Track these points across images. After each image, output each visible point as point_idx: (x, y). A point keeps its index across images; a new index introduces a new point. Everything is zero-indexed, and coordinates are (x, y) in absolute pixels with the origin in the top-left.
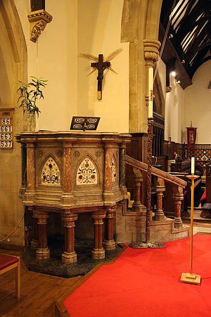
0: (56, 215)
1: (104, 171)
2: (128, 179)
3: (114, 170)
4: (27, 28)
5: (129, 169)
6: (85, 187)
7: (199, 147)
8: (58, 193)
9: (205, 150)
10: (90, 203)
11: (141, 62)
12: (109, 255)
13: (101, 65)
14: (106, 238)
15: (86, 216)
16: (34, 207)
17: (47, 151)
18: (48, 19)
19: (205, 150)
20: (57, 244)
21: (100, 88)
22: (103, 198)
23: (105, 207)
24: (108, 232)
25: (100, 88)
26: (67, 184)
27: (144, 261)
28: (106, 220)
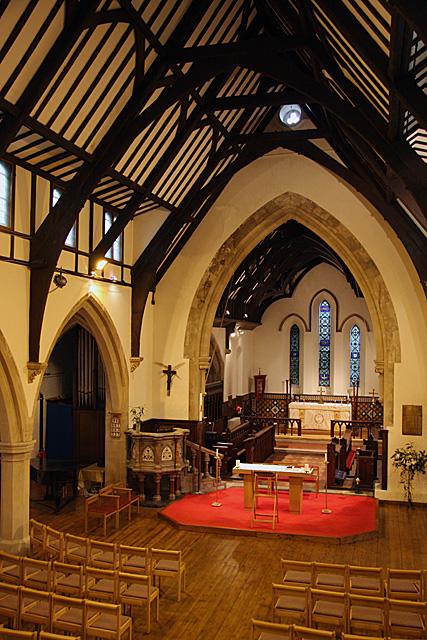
0: (151, 476)
1: (176, 453)
2: (188, 454)
3: (180, 450)
4: (129, 365)
5: (189, 448)
6: (165, 462)
7: (270, 397)
8: (153, 465)
9: (275, 400)
10: (169, 470)
11: (197, 373)
12: (177, 498)
13: (170, 372)
14: (176, 489)
15: (166, 476)
16: (139, 472)
17: (146, 443)
18: (142, 359)
19: (275, 400)
20: (150, 494)
21: (169, 388)
22: (175, 467)
23: (176, 472)
24: (177, 486)
25: (169, 388)
26: (157, 460)
27: (196, 499)
28: (176, 478)
